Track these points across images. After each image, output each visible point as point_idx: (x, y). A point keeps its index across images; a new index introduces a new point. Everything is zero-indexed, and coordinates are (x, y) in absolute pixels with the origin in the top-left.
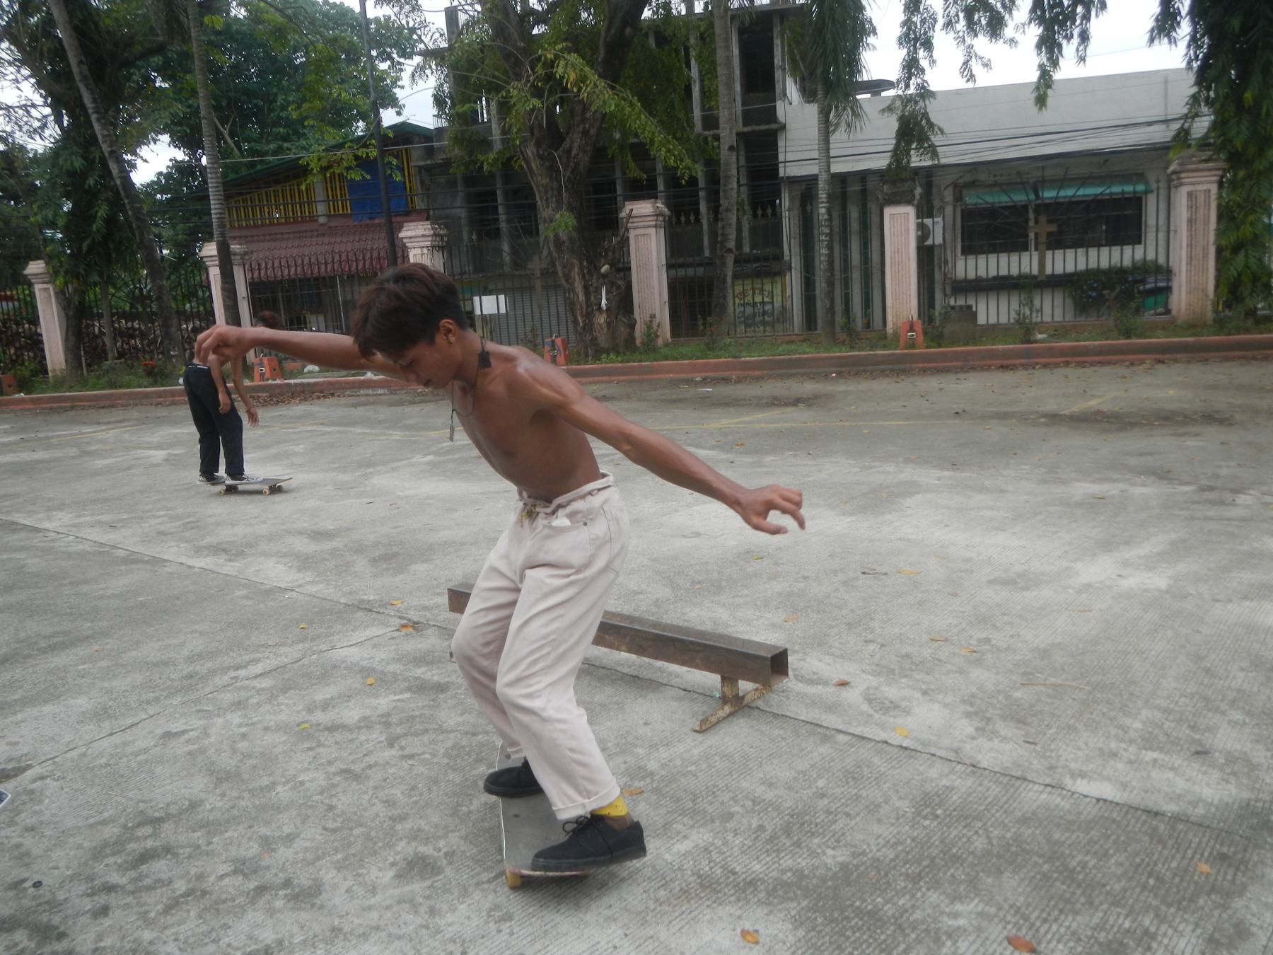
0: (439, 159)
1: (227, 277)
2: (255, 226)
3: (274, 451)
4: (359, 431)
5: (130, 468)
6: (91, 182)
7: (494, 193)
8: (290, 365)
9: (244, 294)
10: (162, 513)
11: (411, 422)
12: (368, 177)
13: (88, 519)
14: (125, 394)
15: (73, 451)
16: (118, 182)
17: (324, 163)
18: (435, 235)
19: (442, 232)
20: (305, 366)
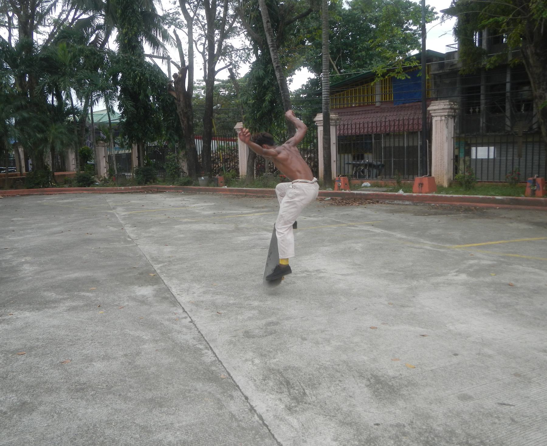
0: (447, 69)
1: (327, 132)
2: (344, 108)
3: (342, 246)
4: (399, 235)
5: (254, 247)
6: (266, 82)
7: (479, 88)
8: (356, 181)
9: (335, 142)
10: (256, 303)
11: (434, 232)
12: (409, 77)
13: (208, 298)
14: (270, 191)
15: (232, 226)
16: (279, 82)
17: (385, 70)
18: (451, 108)
19: (455, 107)
20: (363, 183)
